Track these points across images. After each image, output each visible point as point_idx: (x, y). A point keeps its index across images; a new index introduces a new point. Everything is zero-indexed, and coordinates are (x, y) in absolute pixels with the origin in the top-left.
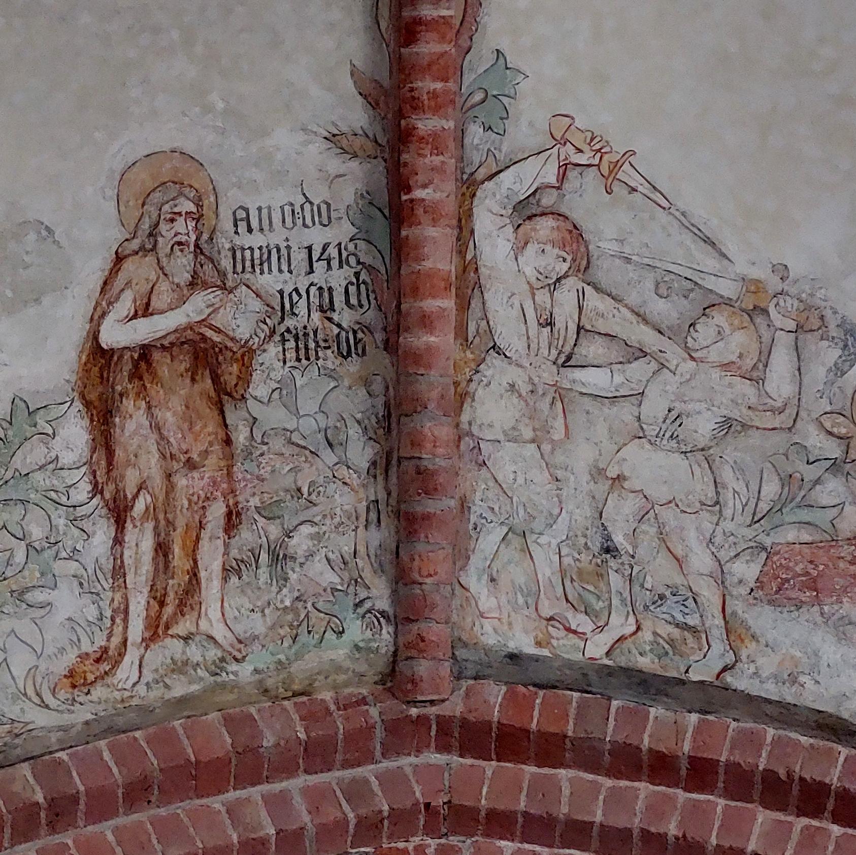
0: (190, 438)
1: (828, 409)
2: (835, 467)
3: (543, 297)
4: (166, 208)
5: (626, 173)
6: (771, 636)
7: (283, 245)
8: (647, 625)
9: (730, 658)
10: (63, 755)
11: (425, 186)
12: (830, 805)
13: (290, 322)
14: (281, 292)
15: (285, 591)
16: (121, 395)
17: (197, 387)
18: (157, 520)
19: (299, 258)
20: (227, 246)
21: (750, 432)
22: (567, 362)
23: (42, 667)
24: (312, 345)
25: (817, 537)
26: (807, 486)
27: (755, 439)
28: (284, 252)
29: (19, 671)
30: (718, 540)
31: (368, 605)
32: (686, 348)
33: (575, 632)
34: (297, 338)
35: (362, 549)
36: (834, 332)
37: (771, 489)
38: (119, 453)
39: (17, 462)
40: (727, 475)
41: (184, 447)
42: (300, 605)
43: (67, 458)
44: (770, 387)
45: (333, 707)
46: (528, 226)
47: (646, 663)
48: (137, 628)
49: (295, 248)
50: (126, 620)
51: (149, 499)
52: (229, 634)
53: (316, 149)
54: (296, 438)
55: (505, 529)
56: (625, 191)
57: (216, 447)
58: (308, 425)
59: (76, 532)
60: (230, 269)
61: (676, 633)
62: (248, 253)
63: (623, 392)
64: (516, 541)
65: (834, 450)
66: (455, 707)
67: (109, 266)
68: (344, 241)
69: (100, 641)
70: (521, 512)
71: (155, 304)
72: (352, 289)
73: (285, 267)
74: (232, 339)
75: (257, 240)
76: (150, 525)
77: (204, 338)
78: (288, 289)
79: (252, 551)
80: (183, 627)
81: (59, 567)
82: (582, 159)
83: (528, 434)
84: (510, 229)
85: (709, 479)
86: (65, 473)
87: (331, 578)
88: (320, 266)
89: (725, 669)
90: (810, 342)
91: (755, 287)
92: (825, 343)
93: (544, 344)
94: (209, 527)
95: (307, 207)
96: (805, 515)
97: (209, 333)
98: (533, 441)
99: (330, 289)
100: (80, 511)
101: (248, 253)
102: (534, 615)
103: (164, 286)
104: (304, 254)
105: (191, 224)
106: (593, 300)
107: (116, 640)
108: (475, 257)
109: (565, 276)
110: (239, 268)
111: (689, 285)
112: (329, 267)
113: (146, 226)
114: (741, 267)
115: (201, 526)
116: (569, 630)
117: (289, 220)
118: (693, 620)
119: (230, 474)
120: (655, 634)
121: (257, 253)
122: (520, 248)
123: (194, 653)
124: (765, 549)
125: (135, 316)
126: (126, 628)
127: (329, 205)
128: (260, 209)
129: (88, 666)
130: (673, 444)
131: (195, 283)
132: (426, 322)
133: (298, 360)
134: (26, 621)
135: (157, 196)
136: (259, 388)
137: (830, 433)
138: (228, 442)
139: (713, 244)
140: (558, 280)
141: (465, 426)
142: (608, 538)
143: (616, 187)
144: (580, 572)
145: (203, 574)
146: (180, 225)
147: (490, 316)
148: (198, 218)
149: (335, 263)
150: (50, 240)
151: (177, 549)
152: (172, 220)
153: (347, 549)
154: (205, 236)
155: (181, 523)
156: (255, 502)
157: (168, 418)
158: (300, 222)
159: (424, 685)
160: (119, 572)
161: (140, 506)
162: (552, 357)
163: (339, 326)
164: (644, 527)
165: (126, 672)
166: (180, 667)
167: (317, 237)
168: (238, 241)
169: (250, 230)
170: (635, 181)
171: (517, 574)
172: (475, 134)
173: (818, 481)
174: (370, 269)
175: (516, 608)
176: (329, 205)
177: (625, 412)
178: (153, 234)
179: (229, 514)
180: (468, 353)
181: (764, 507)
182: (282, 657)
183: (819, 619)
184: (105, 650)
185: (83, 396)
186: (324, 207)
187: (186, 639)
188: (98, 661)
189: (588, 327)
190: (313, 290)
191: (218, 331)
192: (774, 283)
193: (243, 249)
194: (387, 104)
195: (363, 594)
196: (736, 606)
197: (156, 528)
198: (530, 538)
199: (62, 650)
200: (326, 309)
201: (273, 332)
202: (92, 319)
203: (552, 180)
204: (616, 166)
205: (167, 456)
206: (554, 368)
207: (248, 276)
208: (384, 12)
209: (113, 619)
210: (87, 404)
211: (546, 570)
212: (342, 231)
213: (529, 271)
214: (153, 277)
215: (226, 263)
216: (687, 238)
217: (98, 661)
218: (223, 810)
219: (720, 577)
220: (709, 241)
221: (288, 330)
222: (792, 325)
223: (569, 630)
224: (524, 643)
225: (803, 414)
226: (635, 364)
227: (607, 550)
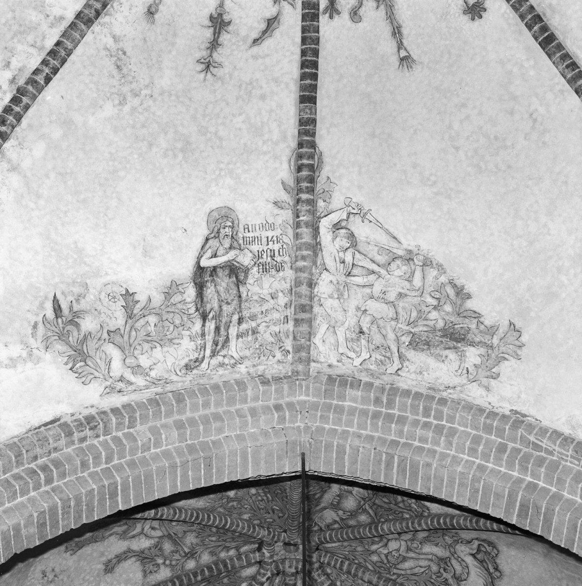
0: (228, 295)
1: (433, 290)
3: (341, 254)
4: (223, 224)
5: (368, 216)
6: (413, 360)
7: (259, 236)
8: (373, 355)
9: (400, 366)
10: (183, 391)
11: (304, 216)
12: (433, 413)
13: (261, 260)
14: (258, 251)
15: (257, 343)
16: (206, 281)
17: (231, 280)
18: (216, 319)
19: (264, 240)
20: (242, 236)
21: (408, 297)
22: (349, 274)
23: (177, 363)
24: (268, 267)
25: (429, 329)
26: (426, 313)
28: (259, 238)
29: (169, 364)
30: (397, 330)
31: (283, 348)
32: (387, 271)
33: (350, 358)
34: (263, 265)
35: (282, 330)
36: (435, 266)
37: (414, 314)
38: (205, 299)
39: (172, 300)
40: (400, 310)
41: (226, 298)
42: (261, 347)
43: (188, 300)
44: (414, 283)
45: (271, 380)
46: (337, 231)
48: (208, 352)
49: (263, 237)
50: (205, 350)
51: (214, 313)
52: (238, 356)
53: (271, 206)
54: (262, 296)
55: (328, 326)
56: (368, 222)
57: (236, 298)
58: (265, 292)
59: (190, 322)
60: (242, 243)
61: (383, 358)
62: (248, 239)
63: (367, 284)
64: (331, 329)
65: (434, 302)
67: (204, 241)
68: (279, 235)
69: (196, 355)
70: (333, 320)
71: (218, 254)
72: (281, 250)
73: (260, 243)
74: (242, 265)
75: (251, 235)
76: (214, 321)
77: (233, 265)
78: (260, 250)
79: (246, 330)
80: (223, 353)
81: (183, 332)
82: (355, 211)
83: (336, 296)
84: (331, 233)
85: (394, 311)
86: (187, 304)
87: (272, 339)
88: (271, 243)
89: (398, 370)
92: (432, 270)
93: (342, 269)
94: (233, 322)
95: (267, 224)
96: (425, 322)
97: (235, 263)
98: (338, 298)
99: (274, 250)
100: (191, 316)
101: (248, 239)
102: (337, 353)
103: (221, 248)
104: (266, 239)
105: (230, 229)
106: (357, 255)
107: (201, 356)
108: (320, 241)
109: (349, 248)
110: (245, 243)
111: (388, 251)
112: (274, 243)
113: (216, 230)
114: (405, 246)
115: (230, 322)
116: (348, 357)
117: (261, 229)
118: (388, 354)
119: (240, 307)
120: (376, 359)
121: (251, 239)
122: (334, 239)
123: (226, 361)
124: (412, 333)
125: (212, 257)
126: (205, 352)
127: (274, 224)
128: (252, 225)
129: (192, 363)
130: (383, 300)
131: (231, 248)
133: (263, 272)
134: (172, 349)
135: (220, 221)
136: (250, 280)
137: (434, 297)
138: (240, 297)
139: (396, 239)
140: (347, 249)
141: (316, 293)
142: (361, 329)
143: (365, 220)
144: (352, 339)
145: (230, 337)
146: (227, 229)
147: (324, 259)
148: (233, 228)
149: (275, 242)
150: (185, 233)
151: (222, 329)
152: (224, 228)
153: (278, 330)
154: (235, 233)
155: (224, 321)
156: (248, 315)
157: (221, 289)
158: (265, 229)
159: (301, 373)
160: (203, 335)
161: (211, 316)
162: (344, 273)
163: (276, 261)
164: (373, 326)
165: (204, 365)
167: (270, 234)
168: (245, 235)
169: (249, 232)
170: (371, 219)
171: (331, 339)
172: (321, 204)
173: (429, 312)
174: (287, 244)
175: (330, 349)
176: (274, 224)
178: (218, 232)
179: (239, 319)
180: (318, 271)
181: (412, 320)
182: (255, 363)
183: (430, 355)
184: (197, 359)
185: (194, 281)
186: (272, 225)
187: (224, 356)
188: (195, 362)
189: (356, 264)
190: (268, 250)
191: (238, 263)
192: (415, 250)
194: (293, 192)
195: (282, 345)
196: (402, 350)
197: (216, 322)
198: (336, 328)
199: (183, 358)
200: (272, 257)
201: (255, 263)
202: (198, 258)
203: (345, 217)
204: (366, 214)
205: (220, 301)
206: (345, 276)
207: (247, 246)
208: (292, 163)
209: (201, 350)
210: (195, 284)
211: (341, 339)
213: (337, 247)
214: (218, 245)
215: (241, 242)
216: (388, 237)
217: (195, 362)
218: (234, 411)
219: (397, 340)
220: (394, 238)
221: (260, 263)
222: (421, 264)
223: (348, 357)
225: (425, 291)
226: (371, 276)
227: (361, 333)
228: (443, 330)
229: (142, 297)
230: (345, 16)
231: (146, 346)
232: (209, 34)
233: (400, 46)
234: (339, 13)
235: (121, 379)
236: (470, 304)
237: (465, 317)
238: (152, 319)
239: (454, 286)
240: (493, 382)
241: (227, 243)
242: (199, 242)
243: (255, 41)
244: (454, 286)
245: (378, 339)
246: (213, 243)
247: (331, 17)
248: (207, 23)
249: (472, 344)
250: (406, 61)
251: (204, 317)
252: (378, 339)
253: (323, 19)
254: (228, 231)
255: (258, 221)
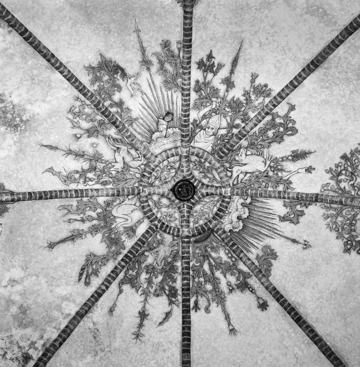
230: (203, 310)
232: (138, 320)
233: (229, 324)
234: (199, 309)
243: (161, 324)
247: (196, 311)
248: (137, 315)
250: (233, 331)
253: (192, 312)
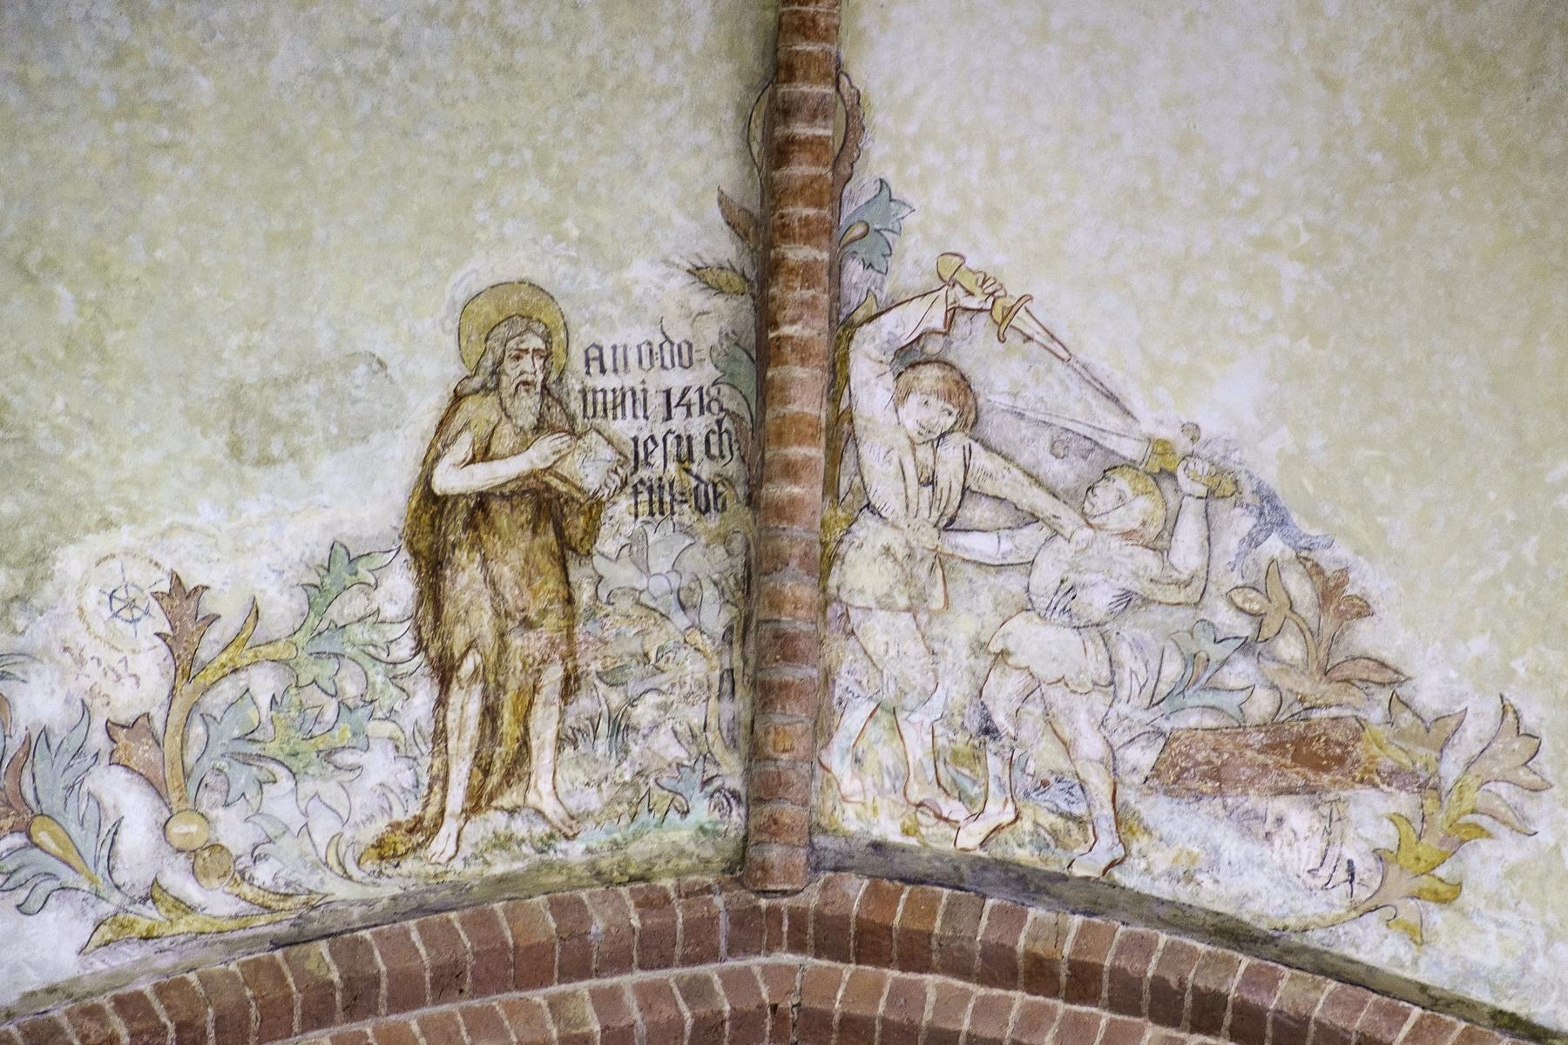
0: (528, 595)
1: (1240, 582)
2: (1246, 646)
3: (924, 453)
4: (512, 344)
5: (1021, 321)
6: (1164, 830)
7: (639, 388)
8: (1027, 813)
9: (1119, 852)
10: (366, 934)
11: (793, 322)
12: (1228, 1019)
13: (644, 473)
14: (635, 440)
15: (625, 765)
16: (454, 546)
17: (538, 541)
18: (485, 681)
19: (656, 402)
20: (578, 387)
21: (1153, 607)
22: (949, 525)
23: (348, 834)
24: (667, 498)
25: (1223, 722)
26: (1213, 666)
27: (1157, 614)
28: (640, 395)
29: (321, 838)
30: (1112, 723)
31: (717, 783)
32: (1083, 514)
33: (946, 820)
34: (651, 490)
35: (713, 722)
36: (1248, 497)
37: (1173, 669)
38: (449, 609)
39: (333, 613)
40: (1124, 653)
41: (521, 604)
42: (641, 781)
43: (390, 611)
44: (1176, 557)
45: (673, 895)
46: (910, 375)
47: (1024, 855)
48: (456, 798)
49: (652, 391)
50: (445, 789)
51: (478, 659)
52: (560, 810)
53: (678, 282)
54: (645, 598)
55: (873, 705)
56: (1019, 340)
57: (557, 606)
58: (659, 585)
59: (395, 691)
60: (579, 413)
61: (1059, 823)
62: (600, 396)
63: (1010, 560)
64: (885, 719)
65: (1245, 628)
66: (811, 898)
67: (446, 404)
68: (707, 384)
69: (415, 809)
70: (892, 686)
71: (496, 448)
72: (714, 439)
73: (640, 413)
74: (580, 489)
75: (610, 382)
76: (478, 688)
77: (548, 488)
78: (644, 436)
79: (591, 719)
80: (509, 799)
81: (373, 727)
82: (973, 303)
83: (903, 601)
84: (889, 378)
85: (1103, 657)
86: (386, 627)
87: (677, 752)
88: (679, 413)
89: (1112, 864)
90: (1220, 508)
91: (1161, 447)
92: (1238, 511)
93: (925, 504)
94: (544, 691)
95: (667, 346)
96: (1210, 698)
97: (555, 482)
98: (908, 610)
99: (689, 438)
100: (401, 669)
101: (600, 396)
102: (902, 801)
103: (506, 429)
104: (661, 399)
105: (539, 363)
106: (981, 459)
107: (432, 810)
108: (850, 406)
109: (951, 431)
110: (590, 412)
111: (1088, 444)
112: (689, 414)
113: (488, 363)
114: (1147, 426)
115: (535, 690)
116: (939, 817)
117: (646, 361)
118: (1079, 810)
119: (570, 636)
120: (1036, 824)
121: (610, 397)
122: (900, 399)
123: (520, 827)
124: (1162, 734)
125: (473, 461)
126: (444, 797)
127: (690, 346)
128: (614, 348)
129: (399, 835)
130: (1065, 618)
131: (541, 427)
132: (791, 471)
133: (652, 514)
134: (333, 784)
135: (502, 331)
136: (607, 543)
137: (1242, 610)
138: (570, 600)
139: (1116, 401)
140: (942, 435)
141: (832, 591)
142: (988, 718)
143: (1010, 335)
144: (955, 754)
145: (534, 743)
146: (526, 363)
147: (865, 472)
148: (547, 356)
149: (695, 409)
150: (381, 375)
151: (507, 715)
152: (518, 358)
153: (697, 721)
154: (554, 376)
155: (512, 686)
156: (596, 666)
157: (505, 573)
158: (658, 363)
159: (776, 873)
160: (440, 736)
161: (468, 667)
162: (933, 519)
163: (697, 478)
164: (1029, 707)
165: (442, 844)
166: (503, 842)
167: (676, 380)
168: (589, 382)
169: (603, 371)
170: (1031, 328)
171: (883, 754)
172: (854, 272)
173: (1225, 662)
174: (734, 416)
175: (881, 791)
176: (690, 346)
177: (1013, 583)
178: (497, 371)
179: (567, 679)
180: (839, 512)
181: (1164, 689)
182: (618, 836)
183: (1221, 813)
184: (419, 820)
185: (410, 544)
186: (685, 348)
187: (512, 812)
188: (411, 831)
189: (974, 488)
190: (670, 438)
191: (565, 480)
192: (1183, 444)
193: (595, 392)
194: (756, 234)
195: (712, 771)
196: (1128, 795)
197: (484, 690)
198: (901, 716)
199: (371, 818)
200: (685, 460)
201: (625, 483)
202: (424, 462)
203: (938, 322)
204: (1010, 312)
205: (501, 614)
206: (935, 532)
207: (598, 421)
208: (757, 133)
209: (430, 787)
210: (415, 554)
211: (917, 748)
212: (704, 374)
213: (911, 424)
214: (494, 418)
215: (575, 406)
216: (1089, 394)
217: (411, 831)
218: (544, 1003)
219: (1112, 763)
220: (1111, 397)
221: (641, 482)
222: (1202, 491)
223: (939, 817)
224: (889, 829)
225: (1212, 588)
226: (1026, 531)
227: (987, 731)
228: (1271, 726)
229: (228, 607)
231: (242, 777)
235: (154, 893)
236: (1366, 637)
237: (1347, 680)
238: (264, 683)
239: (1314, 571)
240: (1438, 918)
241: (527, 408)
242: (427, 408)
244: (1314, 571)
245: (1044, 756)
246: (481, 411)
249: (1370, 777)
251: (444, 672)
252: (1044, 756)
254: (530, 367)
255: (634, 336)
